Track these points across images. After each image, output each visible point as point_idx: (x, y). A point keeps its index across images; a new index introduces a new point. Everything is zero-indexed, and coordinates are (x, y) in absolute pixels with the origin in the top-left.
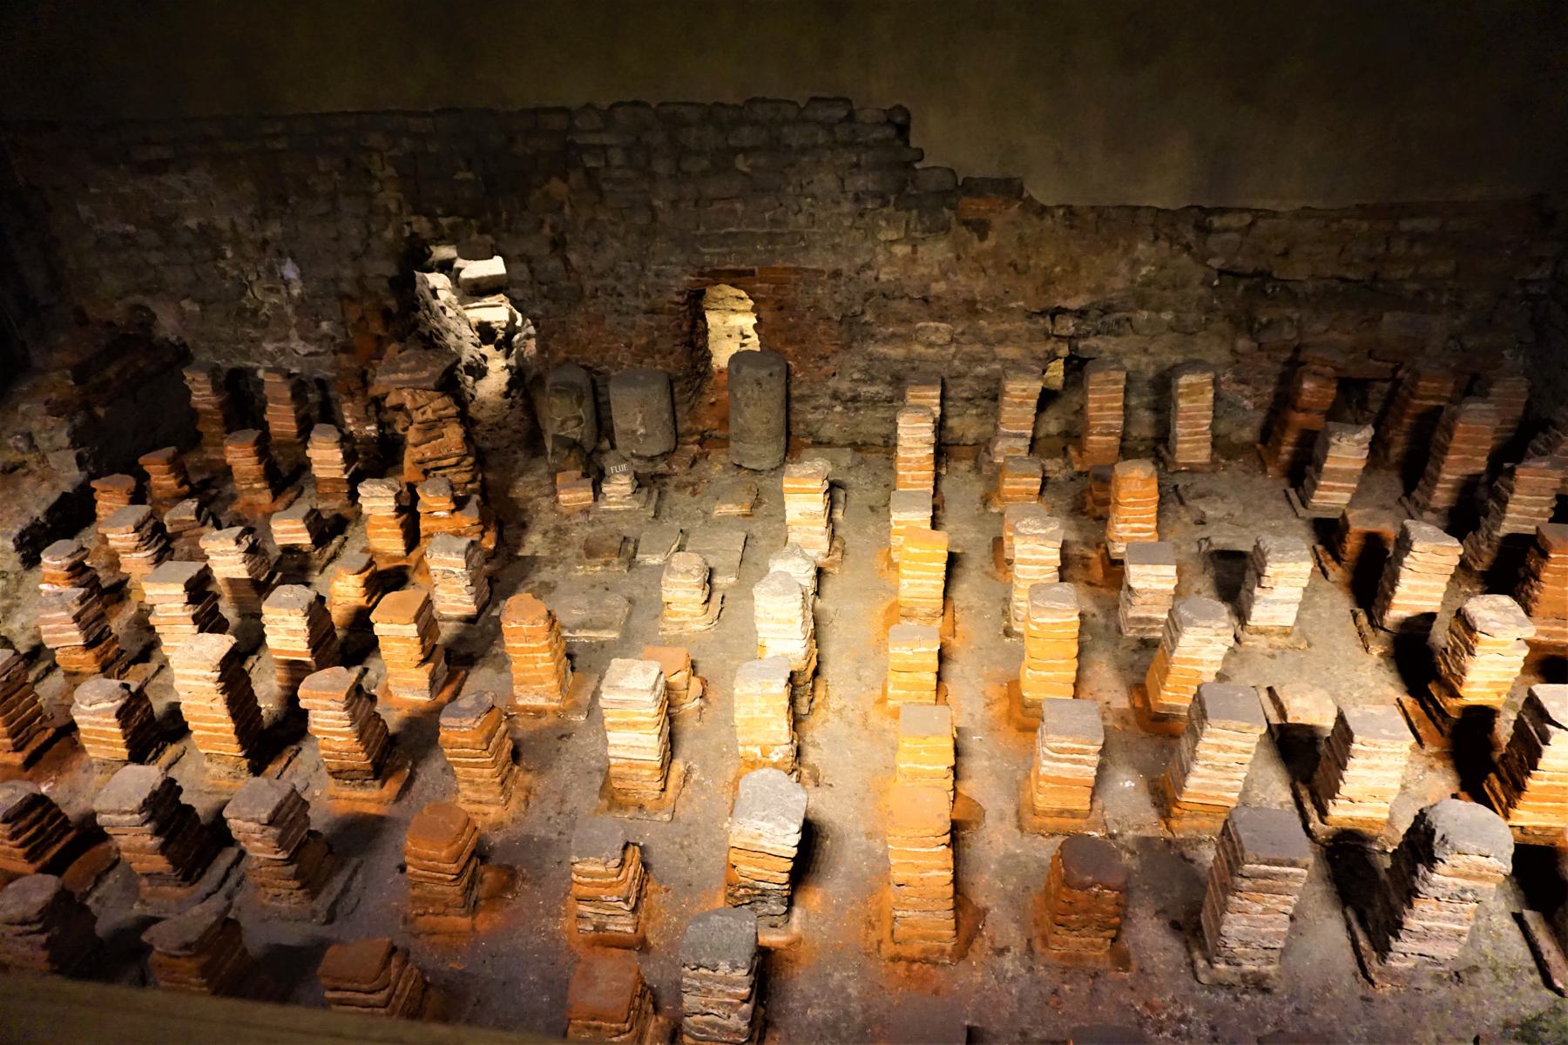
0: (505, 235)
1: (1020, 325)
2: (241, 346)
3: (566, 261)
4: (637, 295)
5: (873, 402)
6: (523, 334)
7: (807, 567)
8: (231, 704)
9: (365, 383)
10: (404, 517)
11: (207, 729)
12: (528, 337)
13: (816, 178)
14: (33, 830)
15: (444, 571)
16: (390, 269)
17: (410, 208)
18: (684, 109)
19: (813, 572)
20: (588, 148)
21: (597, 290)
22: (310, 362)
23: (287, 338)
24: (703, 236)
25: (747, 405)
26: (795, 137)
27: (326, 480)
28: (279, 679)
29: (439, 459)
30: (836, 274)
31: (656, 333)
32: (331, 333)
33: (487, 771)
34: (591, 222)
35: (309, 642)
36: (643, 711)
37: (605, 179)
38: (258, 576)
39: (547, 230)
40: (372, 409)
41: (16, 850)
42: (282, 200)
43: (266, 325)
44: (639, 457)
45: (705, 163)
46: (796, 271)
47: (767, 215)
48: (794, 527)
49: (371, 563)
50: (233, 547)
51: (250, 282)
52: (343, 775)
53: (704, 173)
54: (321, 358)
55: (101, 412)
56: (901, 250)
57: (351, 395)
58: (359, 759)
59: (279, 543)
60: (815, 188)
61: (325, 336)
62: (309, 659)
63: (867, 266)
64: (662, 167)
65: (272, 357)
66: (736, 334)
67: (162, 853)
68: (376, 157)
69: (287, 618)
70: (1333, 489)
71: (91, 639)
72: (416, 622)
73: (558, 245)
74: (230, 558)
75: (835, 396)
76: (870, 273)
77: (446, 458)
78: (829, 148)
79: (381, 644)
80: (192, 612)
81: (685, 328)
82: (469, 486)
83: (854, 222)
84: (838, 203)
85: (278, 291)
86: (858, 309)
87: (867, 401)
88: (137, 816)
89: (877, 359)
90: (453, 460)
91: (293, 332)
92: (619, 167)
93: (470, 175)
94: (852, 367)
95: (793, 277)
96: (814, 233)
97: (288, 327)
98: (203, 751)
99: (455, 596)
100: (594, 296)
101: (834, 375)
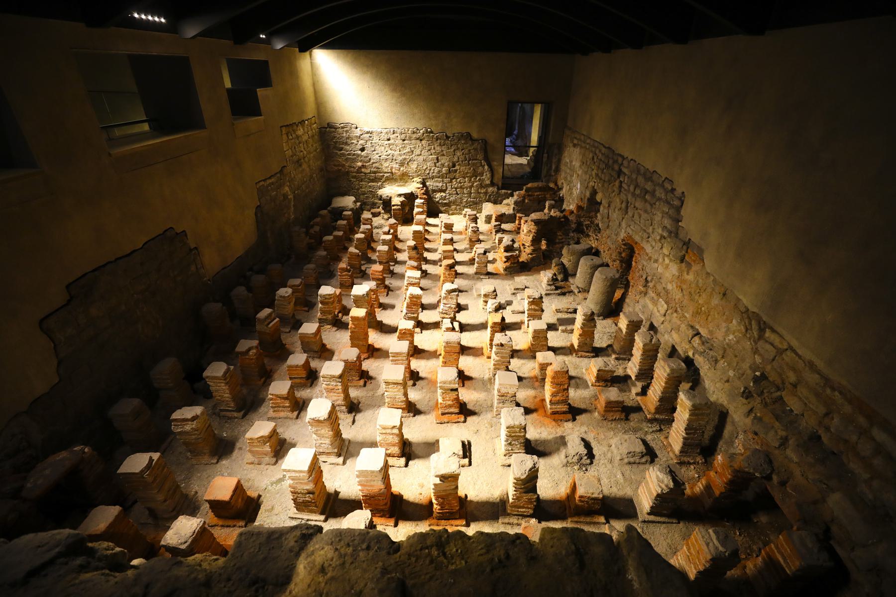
1: (683, 327)
55: (526, 201)
56: (667, 261)
70: (645, 493)
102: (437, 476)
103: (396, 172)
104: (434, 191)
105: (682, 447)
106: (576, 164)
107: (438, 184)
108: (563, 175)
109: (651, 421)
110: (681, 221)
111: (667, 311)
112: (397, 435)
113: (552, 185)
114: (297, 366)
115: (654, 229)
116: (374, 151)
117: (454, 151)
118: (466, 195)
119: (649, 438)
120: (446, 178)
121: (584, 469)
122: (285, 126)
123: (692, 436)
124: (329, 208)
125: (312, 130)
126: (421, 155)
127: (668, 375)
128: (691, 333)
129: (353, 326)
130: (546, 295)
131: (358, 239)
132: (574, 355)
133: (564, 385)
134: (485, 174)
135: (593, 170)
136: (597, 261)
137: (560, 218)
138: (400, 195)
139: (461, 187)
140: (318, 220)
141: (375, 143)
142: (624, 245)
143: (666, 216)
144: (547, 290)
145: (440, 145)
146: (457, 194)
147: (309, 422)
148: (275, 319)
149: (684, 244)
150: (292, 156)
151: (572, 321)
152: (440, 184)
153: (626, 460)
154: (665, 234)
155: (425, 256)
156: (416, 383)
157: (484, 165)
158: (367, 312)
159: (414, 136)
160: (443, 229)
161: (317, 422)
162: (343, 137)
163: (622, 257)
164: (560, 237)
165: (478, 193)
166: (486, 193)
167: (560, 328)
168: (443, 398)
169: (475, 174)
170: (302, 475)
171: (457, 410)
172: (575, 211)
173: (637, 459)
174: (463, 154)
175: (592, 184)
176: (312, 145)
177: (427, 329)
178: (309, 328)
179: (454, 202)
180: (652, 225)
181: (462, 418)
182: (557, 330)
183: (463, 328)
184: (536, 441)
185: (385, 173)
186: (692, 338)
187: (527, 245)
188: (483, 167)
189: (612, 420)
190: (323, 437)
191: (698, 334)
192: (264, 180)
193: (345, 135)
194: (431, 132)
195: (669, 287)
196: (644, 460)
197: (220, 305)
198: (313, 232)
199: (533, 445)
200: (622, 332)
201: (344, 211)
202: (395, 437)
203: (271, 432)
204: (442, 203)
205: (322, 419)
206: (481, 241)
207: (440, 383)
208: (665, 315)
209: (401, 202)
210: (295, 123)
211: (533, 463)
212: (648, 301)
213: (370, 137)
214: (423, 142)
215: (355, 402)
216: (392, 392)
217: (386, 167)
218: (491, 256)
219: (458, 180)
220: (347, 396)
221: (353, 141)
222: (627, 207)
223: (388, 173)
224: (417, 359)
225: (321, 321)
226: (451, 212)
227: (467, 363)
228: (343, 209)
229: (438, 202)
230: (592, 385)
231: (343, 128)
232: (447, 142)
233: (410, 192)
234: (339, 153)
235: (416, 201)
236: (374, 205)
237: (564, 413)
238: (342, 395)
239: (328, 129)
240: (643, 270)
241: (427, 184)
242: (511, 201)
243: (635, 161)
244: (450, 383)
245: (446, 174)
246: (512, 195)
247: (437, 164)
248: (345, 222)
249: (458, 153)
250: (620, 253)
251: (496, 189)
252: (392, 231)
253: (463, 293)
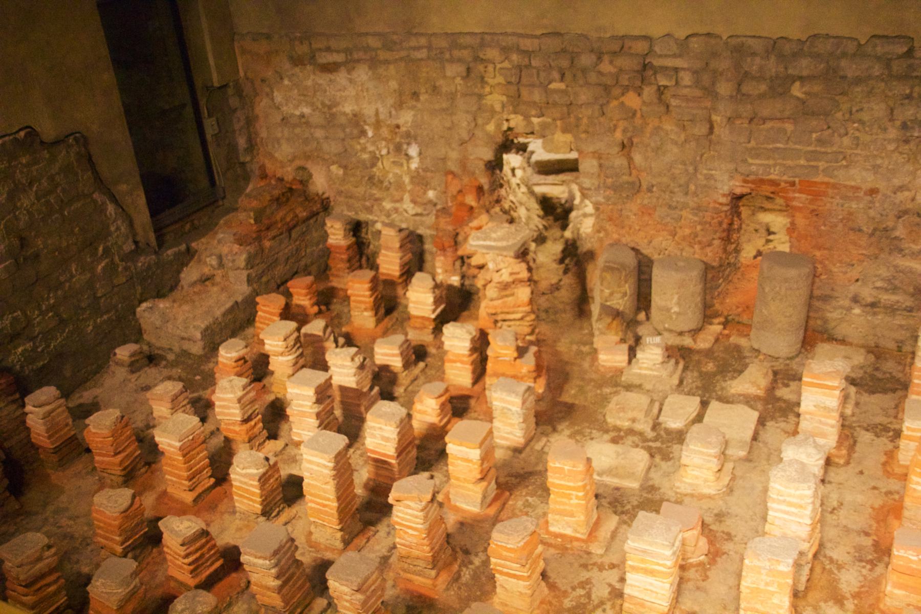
0: (583, 136)
2: (368, 204)
3: (630, 160)
4: (686, 194)
5: (892, 310)
6: (581, 212)
7: (818, 457)
8: (338, 488)
9: (456, 244)
10: (475, 356)
11: (318, 504)
12: (585, 215)
13: (866, 106)
14: (198, 555)
15: (503, 408)
16: (488, 154)
17: (511, 108)
18: (750, 41)
19: (822, 462)
20: (664, 69)
21: (653, 186)
22: (415, 221)
23: (401, 200)
24: (753, 148)
25: (773, 299)
26: (850, 69)
27: (418, 317)
28: (368, 472)
29: (508, 313)
30: (873, 192)
31: (699, 228)
32: (435, 200)
33: (521, 582)
34: (658, 129)
35: (396, 449)
36: (661, 562)
37: (674, 96)
38: (362, 388)
39: (618, 135)
40: (458, 263)
41: (185, 567)
42: (415, 95)
43: (388, 189)
44: (670, 331)
45: (763, 87)
46: (834, 186)
47: (814, 135)
48: (808, 416)
49: (447, 390)
50: (349, 363)
51: (382, 156)
52: (409, 561)
53: (761, 96)
54: (424, 219)
57: (443, 249)
58: (423, 551)
59: (378, 362)
60: (865, 116)
61: (430, 201)
62: (393, 461)
63: (901, 188)
64: (724, 88)
65: (388, 215)
66: (763, 231)
67: (279, 593)
68: (490, 68)
69: (384, 427)
71: (246, 417)
72: (480, 447)
73: (625, 147)
74: (345, 371)
75: (855, 300)
76: (906, 194)
77: (513, 313)
78: (883, 80)
79: (450, 460)
80: (316, 410)
81: (725, 226)
82: (528, 338)
83: (897, 148)
84: (885, 129)
85: (402, 165)
86: (890, 224)
87: (885, 307)
88: (267, 562)
89: (900, 271)
90: (519, 316)
91: (407, 197)
92: (686, 87)
93: (562, 86)
94: (876, 276)
95: (830, 191)
96: (856, 155)
97: (404, 191)
98: (312, 519)
99: (509, 429)
100: (650, 190)
101: (857, 280)
146: (62, 322)
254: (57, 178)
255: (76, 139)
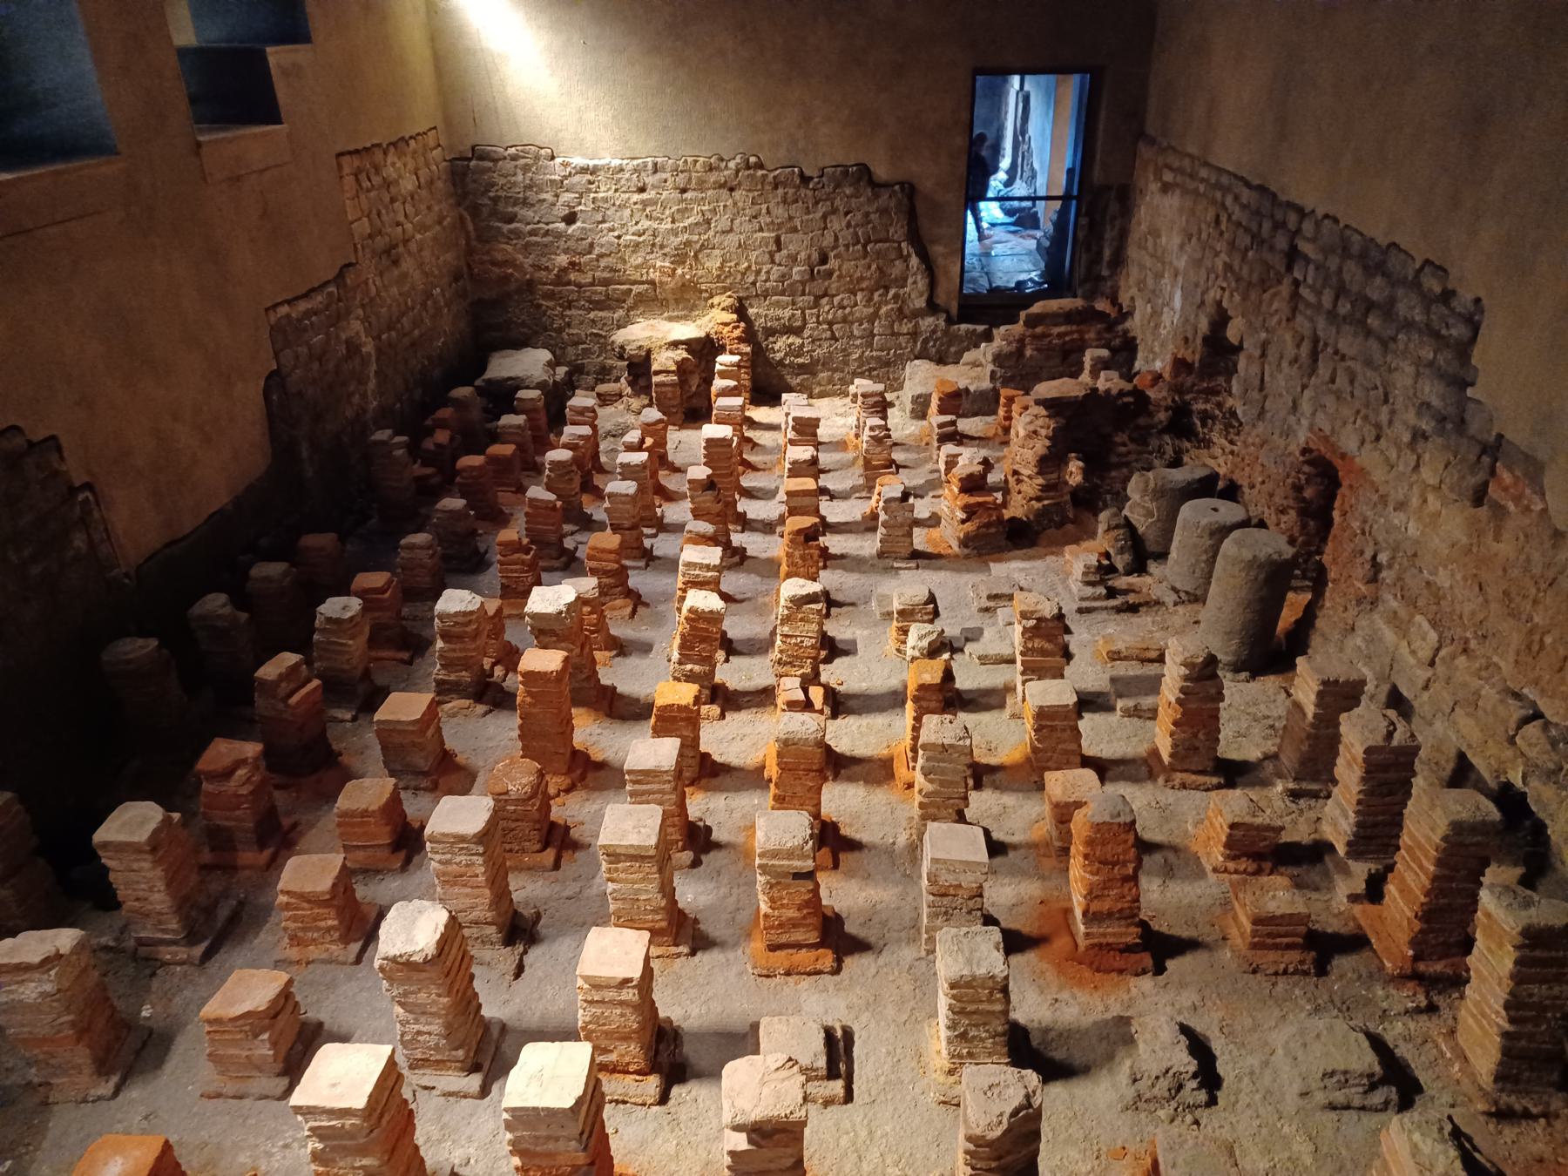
1: (1490, 693)
55: (1028, 352)
56: (1433, 502)
102: (737, 1128)
103: (666, 279)
104: (770, 332)
105: (1501, 1064)
106: (1171, 240)
107: (779, 312)
108: (1134, 272)
109: (1402, 978)
110: (1472, 384)
111: (1438, 650)
112: (636, 1008)
113: (1102, 305)
114: (365, 813)
115: (1393, 412)
116: (603, 221)
117: (824, 217)
118: (858, 342)
119: (1393, 1033)
120: (803, 294)
121: (1189, 1119)
122: (350, 153)
123: (1529, 1027)
124: (478, 382)
125: (427, 165)
126: (731, 230)
127: (1445, 839)
128: (1516, 712)
129: (528, 699)
130: (1080, 611)
131: (556, 465)
132: (1161, 780)
133: (1124, 864)
134: (910, 281)
135: (1217, 254)
136: (1229, 512)
137: (1121, 393)
138: (675, 344)
139: (844, 320)
140: (445, 413)
141: (605, 200)
142: (1307, 462)
143: (1427, 371)
144: (1082, 599)
145: (785, 201)
146: (834, 338)
147: (382, 969)
148: (309, 681)
149: (1484, 451)
150: (370, 236)
151: (1153, 685)
152: (787, 313)
153: (1320, 1097)
154: (1426, 425)
155: (740, 509)
156: (703, 858)
157: (909, 255)
158: (566, 660)
159: (713, 177)
160: (791, 434)
161: (403, 967)
162: (514, 184)
163: (1304, 500)
164: (1122, 449)
165: (893, 334)
166: (914, 335)
167: (1120, 704)
168: (772, 900)
169: (883, 283)
170: (348, 1122)
171: (813, 937)
172: (1167, 376)
173: (1354, 1094)
174: (849, 225)
175: (1214, 294)
176: (429, 208)
177: (738, 708)
178: (404, 706)
179: (826, 363)
180: (1386, 401)
181: (827, 959)
182: (1110, 709)
183: (838, 704)
184: (1047, 1030)
185: (635, 282)
186: (1519, 728)
187: (1026, 472)
188: (906, 259)
189: (1276, 974)
190: (424, 1013)
191: (1538, 715)
192: (288, 302)
193: (520, 178)
194: (760, 166)
195: (1443, 579)
196: (1377, 1098)
197: (154, 643)
198: (432, 447)
199: (1034, 1043)
200: (1304, 715)
201: (518, 388)
202: (628, 1011)
203: (274, 1002)
204: (791, 365)
205: (417, 958)
206: (898, 467)
207: (762, 855)
208: (1432, 664)
209: (677, 363)
210: (379, 145)
211: (1023, 1092)
212: (1381, 624)
213: (590, 183)
214: (737, 194)
215: (527, 912)
216: (626, 881)
217: (637, 267)
218: (922, 508)
219: (836, 300)
220: (501, 895)
221: (544, 196)
222: (1314, 355)
223: (642, 283)
224: (707, 789)
225: (445, 690)
226: (817, 391)
227: (840, 800)
228: (517, 384)
229: (781, 362)
230: (1215, 870)
231: (514, 158)
232: (803, 192)
233: (702, 334)
234: (506, 227)
235: (720, 359)
236: (604, 374)
237: (1129, 949)
238: (487, 892)
239: (473, 163)
240: (1363, 533)
241: (751, 311)
242: (985, 353)
243: (1336, 221)
244: (790, 854)
245: (803, 283)
246: (988, 337)
247: (777, 257)
248: (519, 419)
249: (836, 224)
250: (1298, 488)
251: (942, 323)
252: (649, 441)
253: (845, 609)
254: (872, 216)
255: (902, 189)
